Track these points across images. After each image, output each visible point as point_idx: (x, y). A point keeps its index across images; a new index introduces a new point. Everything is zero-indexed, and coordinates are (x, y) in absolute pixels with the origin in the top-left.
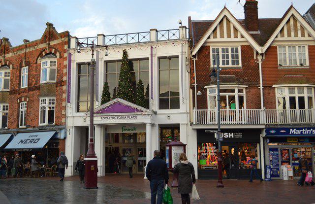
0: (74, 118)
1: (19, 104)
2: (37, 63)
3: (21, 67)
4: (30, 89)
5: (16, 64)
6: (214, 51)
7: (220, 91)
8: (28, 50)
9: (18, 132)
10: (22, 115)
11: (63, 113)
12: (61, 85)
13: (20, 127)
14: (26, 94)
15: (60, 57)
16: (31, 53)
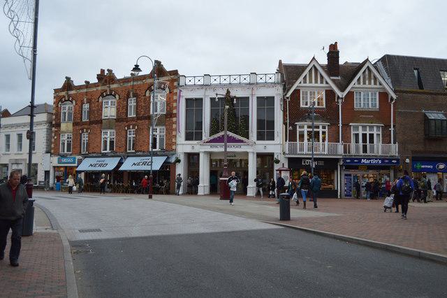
0: (183, 147)
1: (126, 131)
2: (145, 95)
3: (128, 97)
4: (138, 118)
5: (124, 95)
6: (303, 94)
7: (309, 127)
8: (135, 83)
9: (128, 157)
10: (130, 141)
11: (174, 140)
12: (171, 117)
13: (128, 151)
14: (134, 123)
15: (170, 92)
16: (139, 86)
